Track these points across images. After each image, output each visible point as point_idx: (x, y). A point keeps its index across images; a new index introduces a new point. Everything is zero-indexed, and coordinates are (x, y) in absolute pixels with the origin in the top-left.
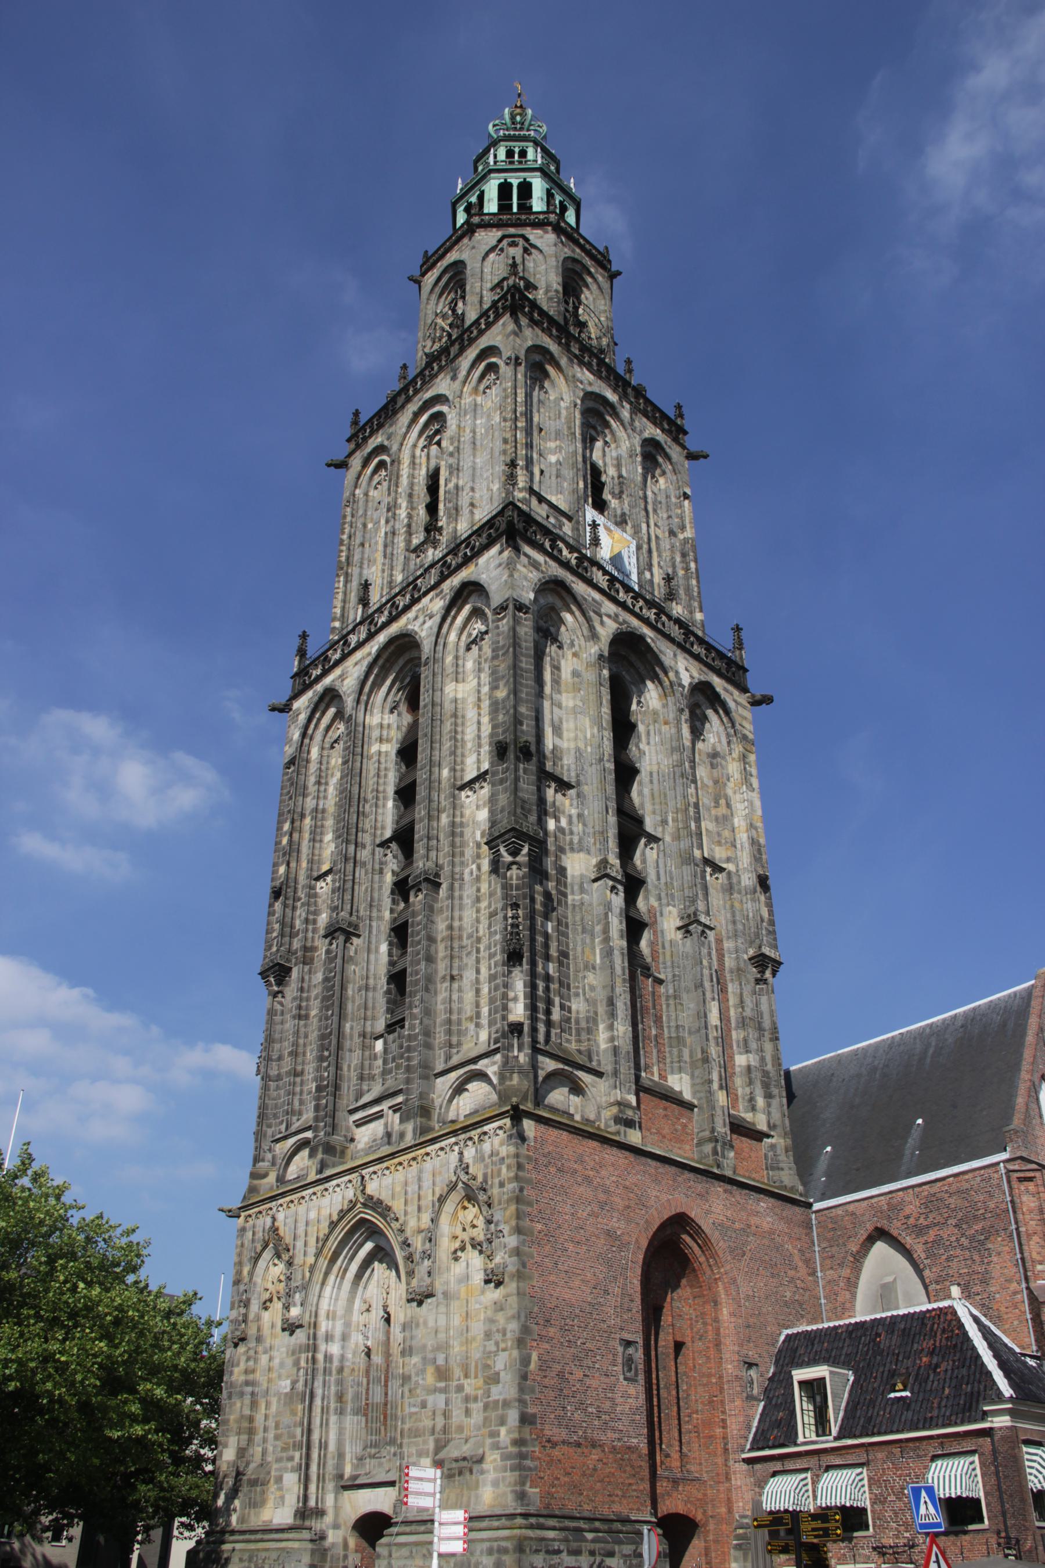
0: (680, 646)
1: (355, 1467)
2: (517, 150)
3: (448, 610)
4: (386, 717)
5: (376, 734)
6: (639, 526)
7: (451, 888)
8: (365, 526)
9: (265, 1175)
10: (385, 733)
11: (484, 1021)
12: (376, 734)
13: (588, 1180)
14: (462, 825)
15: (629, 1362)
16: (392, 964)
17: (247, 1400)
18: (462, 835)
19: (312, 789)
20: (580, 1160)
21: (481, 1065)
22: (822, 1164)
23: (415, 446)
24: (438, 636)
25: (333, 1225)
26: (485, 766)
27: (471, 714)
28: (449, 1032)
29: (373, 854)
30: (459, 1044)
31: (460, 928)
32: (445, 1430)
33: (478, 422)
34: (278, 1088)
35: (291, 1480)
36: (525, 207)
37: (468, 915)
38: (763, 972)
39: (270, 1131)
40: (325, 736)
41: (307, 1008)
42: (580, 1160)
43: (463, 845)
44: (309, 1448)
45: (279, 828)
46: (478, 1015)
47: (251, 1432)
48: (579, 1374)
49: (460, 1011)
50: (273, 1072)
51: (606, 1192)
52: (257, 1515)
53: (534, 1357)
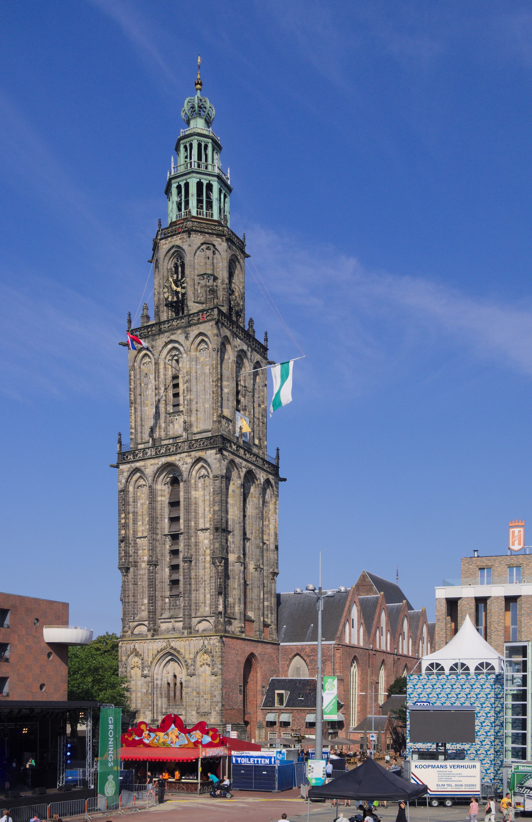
2: (203, 144)
5: (159, 493)
7: (196, 563)
13: (234, 648)
18: (198, 546)
19: (131, 503)
21: (207, 618)
23: (165, 358)
26: (208, 526)
27: (201, 504)
28: (196, 606)
30: (199, 609)
31: (199, 576)
33: (198, 367)
48: (231, 694)
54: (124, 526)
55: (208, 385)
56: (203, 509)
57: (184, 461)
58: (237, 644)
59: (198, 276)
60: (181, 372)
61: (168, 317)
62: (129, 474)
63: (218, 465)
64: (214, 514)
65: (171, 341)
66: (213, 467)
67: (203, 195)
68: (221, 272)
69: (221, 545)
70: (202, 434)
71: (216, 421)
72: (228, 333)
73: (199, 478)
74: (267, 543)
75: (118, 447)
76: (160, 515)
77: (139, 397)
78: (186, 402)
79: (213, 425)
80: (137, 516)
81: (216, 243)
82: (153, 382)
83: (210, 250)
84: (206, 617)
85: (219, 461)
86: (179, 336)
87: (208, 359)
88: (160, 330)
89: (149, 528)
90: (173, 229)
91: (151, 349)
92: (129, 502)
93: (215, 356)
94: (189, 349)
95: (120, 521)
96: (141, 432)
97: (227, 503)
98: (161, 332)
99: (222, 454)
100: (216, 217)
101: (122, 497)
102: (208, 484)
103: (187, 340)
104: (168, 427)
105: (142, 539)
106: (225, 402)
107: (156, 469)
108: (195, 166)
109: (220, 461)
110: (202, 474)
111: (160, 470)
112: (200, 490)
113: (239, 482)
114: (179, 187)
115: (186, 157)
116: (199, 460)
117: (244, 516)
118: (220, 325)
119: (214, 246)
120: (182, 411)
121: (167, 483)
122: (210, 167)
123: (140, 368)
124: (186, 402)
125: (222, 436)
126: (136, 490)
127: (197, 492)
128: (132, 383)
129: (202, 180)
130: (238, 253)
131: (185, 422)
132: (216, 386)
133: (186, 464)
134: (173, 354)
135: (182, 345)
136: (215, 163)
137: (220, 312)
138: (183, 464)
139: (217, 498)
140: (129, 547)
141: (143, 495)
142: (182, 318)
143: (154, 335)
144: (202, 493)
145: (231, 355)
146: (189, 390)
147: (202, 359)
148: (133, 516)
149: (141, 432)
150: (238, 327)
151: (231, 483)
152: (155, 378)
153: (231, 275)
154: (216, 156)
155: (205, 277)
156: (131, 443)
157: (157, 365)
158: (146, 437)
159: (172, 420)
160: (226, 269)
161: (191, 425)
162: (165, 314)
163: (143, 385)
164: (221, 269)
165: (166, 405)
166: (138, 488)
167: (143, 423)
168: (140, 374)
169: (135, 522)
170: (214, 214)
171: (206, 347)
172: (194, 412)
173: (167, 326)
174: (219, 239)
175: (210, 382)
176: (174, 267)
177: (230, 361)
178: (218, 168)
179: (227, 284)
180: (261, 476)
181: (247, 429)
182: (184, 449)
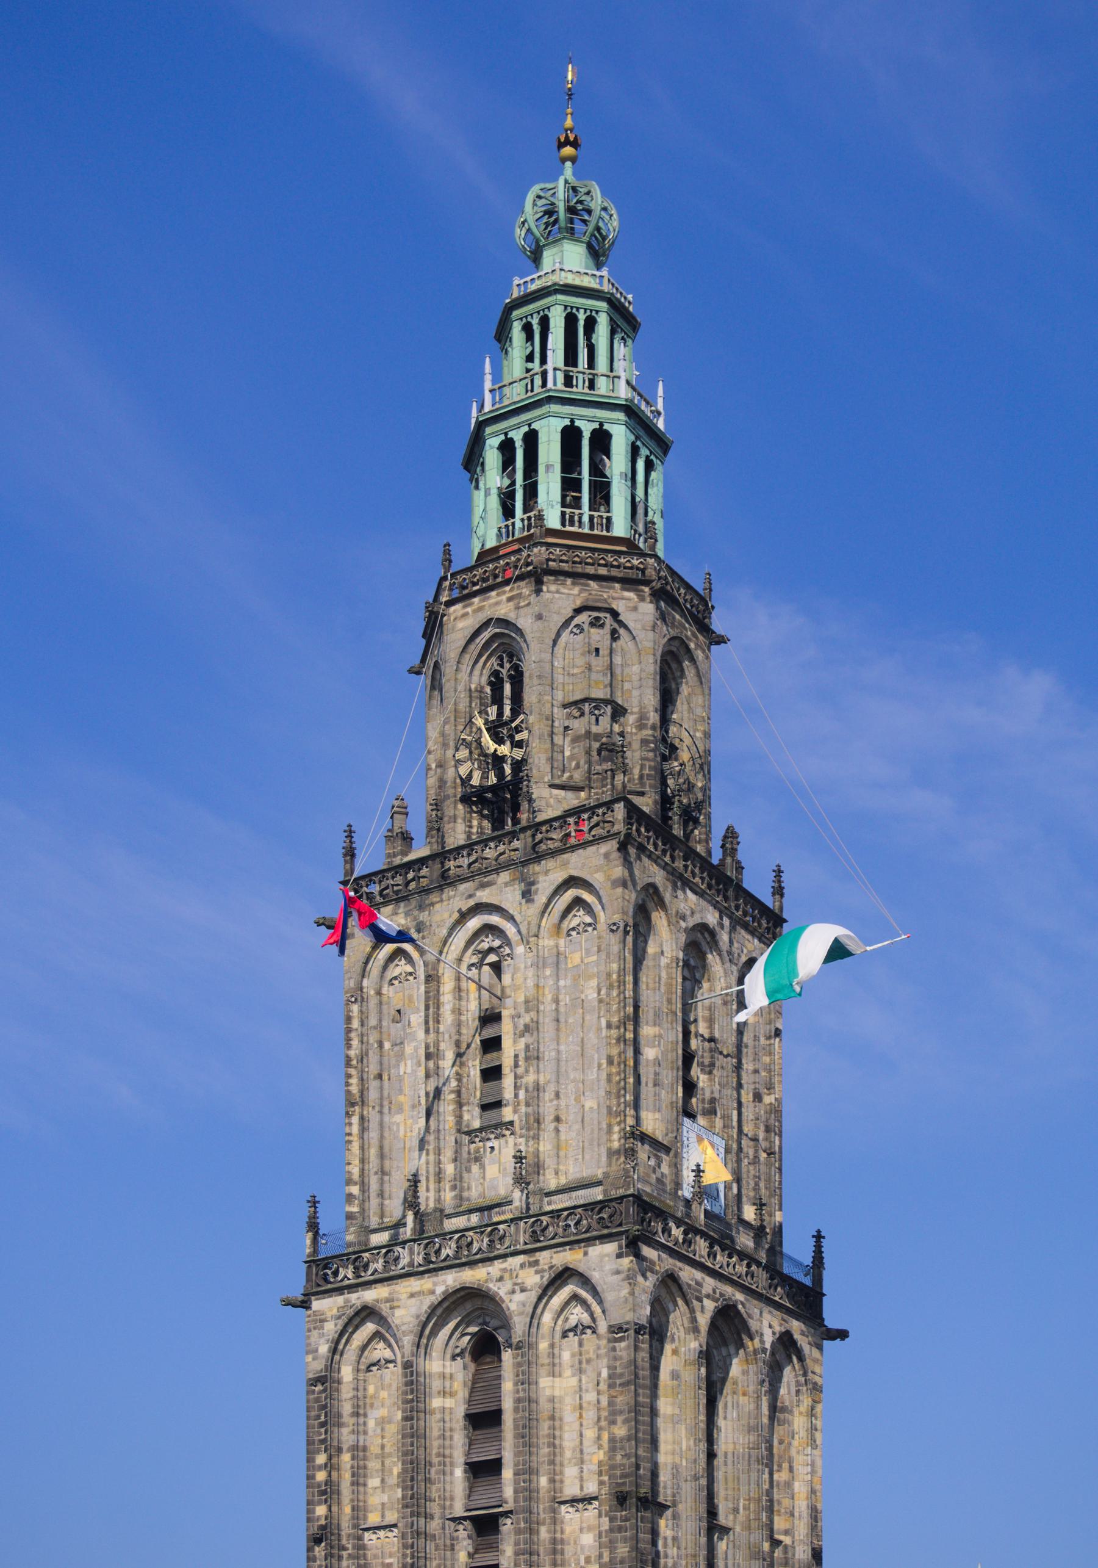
4: (448, 1363)
5: (436, 1385)
6: (730, 1117)
10: (447, 1384)
14: (562, 1541)
18: (562, 1553)
19: (347, 1418)
23: (460, 960)
24: (532, 1317)
27: (569, 1417)
29: (444, 1528)
33: (562, 983)
40: (360, 1357)
45: (310, 1460)
54: (324, 1493)
55: (592, 1038)
56: (576, 1435)
57: (513, 1281)
59: (565, 706)
60: (508, 1002)
61: (469, 835)
62: (340, 1327)
63: (625, 1292)
64: (613, 1449)
65: (479, 908)
66: (609, 1297)
67: (580, 464)
68: (635, 693)
69: (636, 1548)
70: (574, 1194)
71: (618, 1152)
72: (658, 876)
73: (565, 1335)
74: (787, 1540)
75: (308, 1242)
76: (438, 1455)
77: (374, 1085)
78: (522, 1094)
79: (610, 1165)
80: (365, 1459)
81: (619, 606)
82: (421, 1034)
83: (602, 626)
85: (628, 1278)
86: (503, 891)
87: (595, 958)
88: (444, 875)
89: (404, 1497)
90: (490, 571)
91: (415, 936)
92: (339, 1415)
93: (616, 948)
94: (534, 930)
95: (310, 1477)
96: (381, 1195)
97: (654, 1412)
98: (446, 881)
99: (638, 1255)
100: (620, 528)
101: (317, 1400)
102: (592, 1355)
103: (530, 901)
104: (465, 1175)
105: (381, 1533)
106: (647, 1091)
107: (425, 1307)
108: (556, 383)
109: (630, 1278)
110: (573, 1321)
111: (439, 1311)
112: (568, 1372)
113: (694, 1345)
114: (507, 447)
115: (530, 358)
116: (564, 1275)
117: (711, 1455)
118: (632, 851)
119: (615, 614)
120: (511, 1123)
121: (461, 1354)
122: (602, 385)
123: (379, 993)
124: (522, 1094)
125: (637, 1198)
126: (361, 1376)
127: (557, 1380)
128: (355, 1043)
129: (577, 423)
130: (689, 631)
131: (519, 1158)
132: (618, 1040)
133: (523, 1290)
134: (485, 946)
135: (511, 918)
136: (617, 370)
137: (633, 812)
138: (513, 1292)
139: (623, 1400)
140: (340, 1558)
141: (385, 1393)
142: (513, 835)
143: (427, 891)
144: (574, 1381)
145: (666, 943)
146: (533, 1056)
147: (575, 959)
148: (353, 1459)
149: (381, 1195)
150: (690, 854)
151: (668, 1348)
152: (427, 1022)
153: (667, 699)
154: (621, 350)
155: (586, 707)
156: (347, 1228)
157: (433, 984)
158: (395, 1208)
159: (477, 1151)
160: (651, 683)
161: (538, 1167)
162: (461, 827)
163: (387, 1045)
164: (636, 684)
165: (460, 1105)
166: (368, 1370)
167: (387, 1163)
168: (380, 1012)
169: (359, 1478)
170: (614, 520)
171: (588, 920)
172: (549, 1125)
173: (465, 862)
174: (631, 595)
175: (600, 1029)
176: (490, 683)
177: (664, 961)
178: (628, 383)
179: (653, 728)
180: (766, 1323)
181: (717, 1174)
182: (517, 1242)
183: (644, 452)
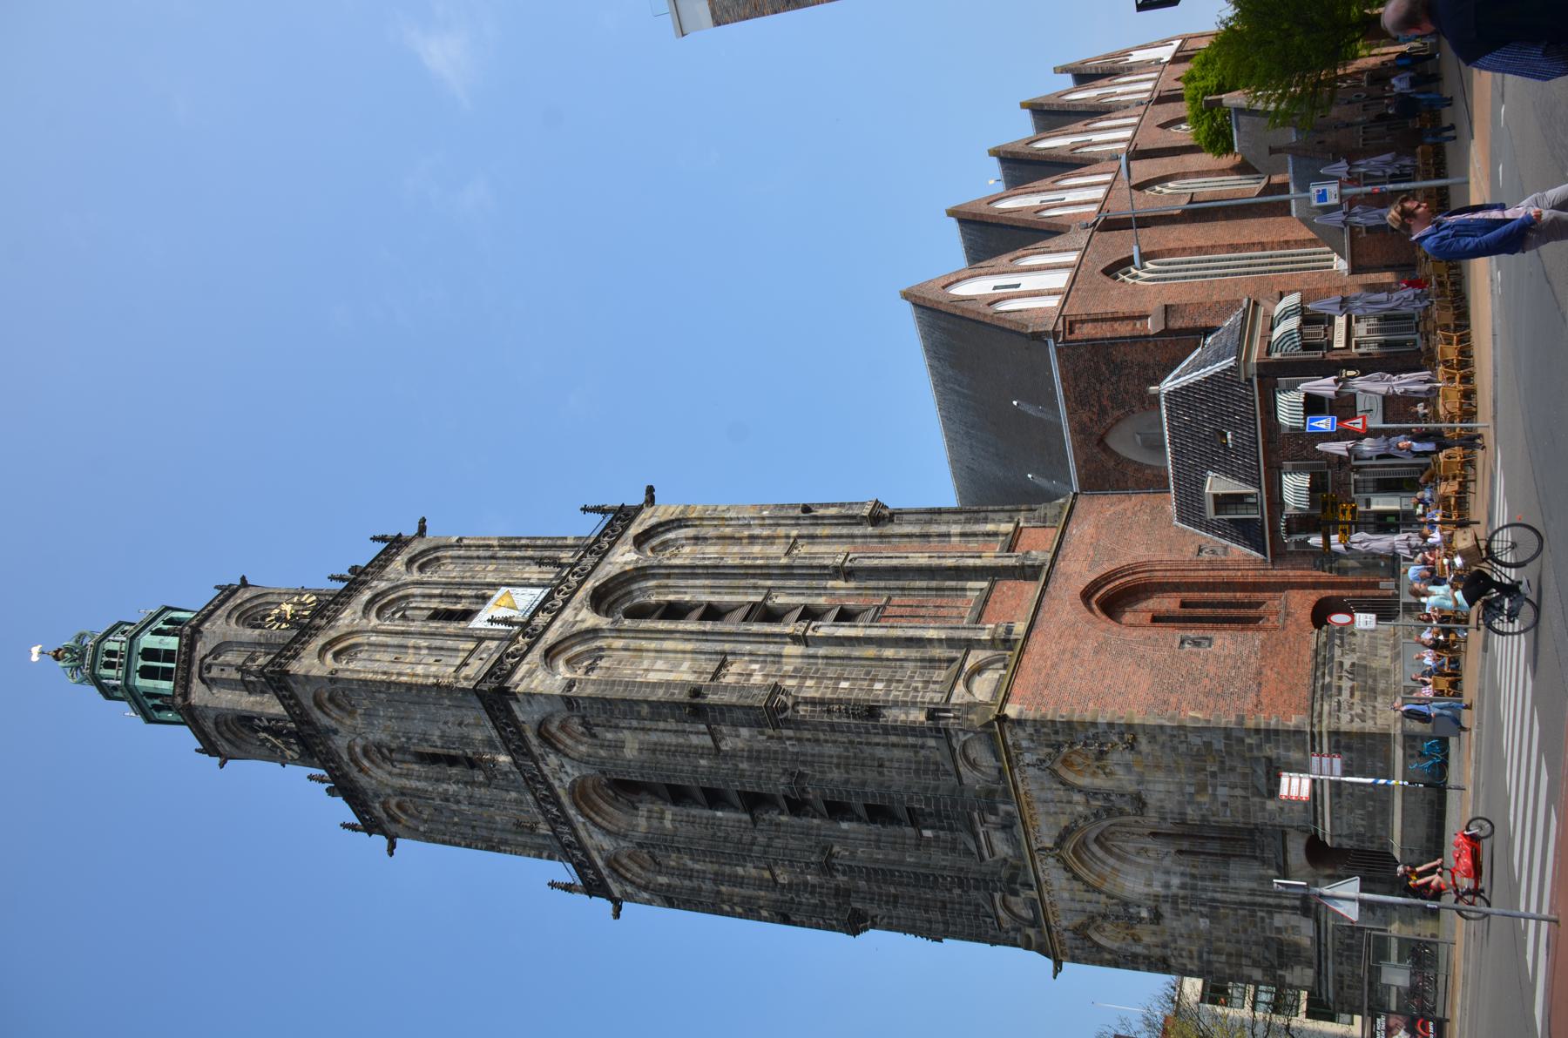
0: (601, 559)
1: (1270, 866)
3: (557, 751)
7: (804, 763)
8: (456, 824)
9: (1028, 937)
11: (920, 741)
12: (655, 823)
13: (1053, 666)
15: (1196, 643)
16: (859, 819)
17: (1214, 958)
18: (759, 751)
19: (695, 883)
20: (1039, 671)
22: (1043, 482)
25: (1076, 877)
27: (654, 737)
30: (936, 763)
31: (839, 757)
32: (1245, 788)
34: (955, 924)
35: (1279, 920)
36: (169, 655)
37: (829, 749)
38: (884, 517)
39: (991, 932)
41: (888, 895)
42: (1039, 671)
43: (768, 750)
44: (1254, 904)
46: (914, 746)
47: (1239, 955)
49: (909, 761)
50: (941, 927)
51: (1064, 651)
52: (1306, 950)
53: (1192, 714)
58: (1042, 655)
84: (952, 750)
133: (562, 766)
144: (626, 732)
183: (160, 625)
